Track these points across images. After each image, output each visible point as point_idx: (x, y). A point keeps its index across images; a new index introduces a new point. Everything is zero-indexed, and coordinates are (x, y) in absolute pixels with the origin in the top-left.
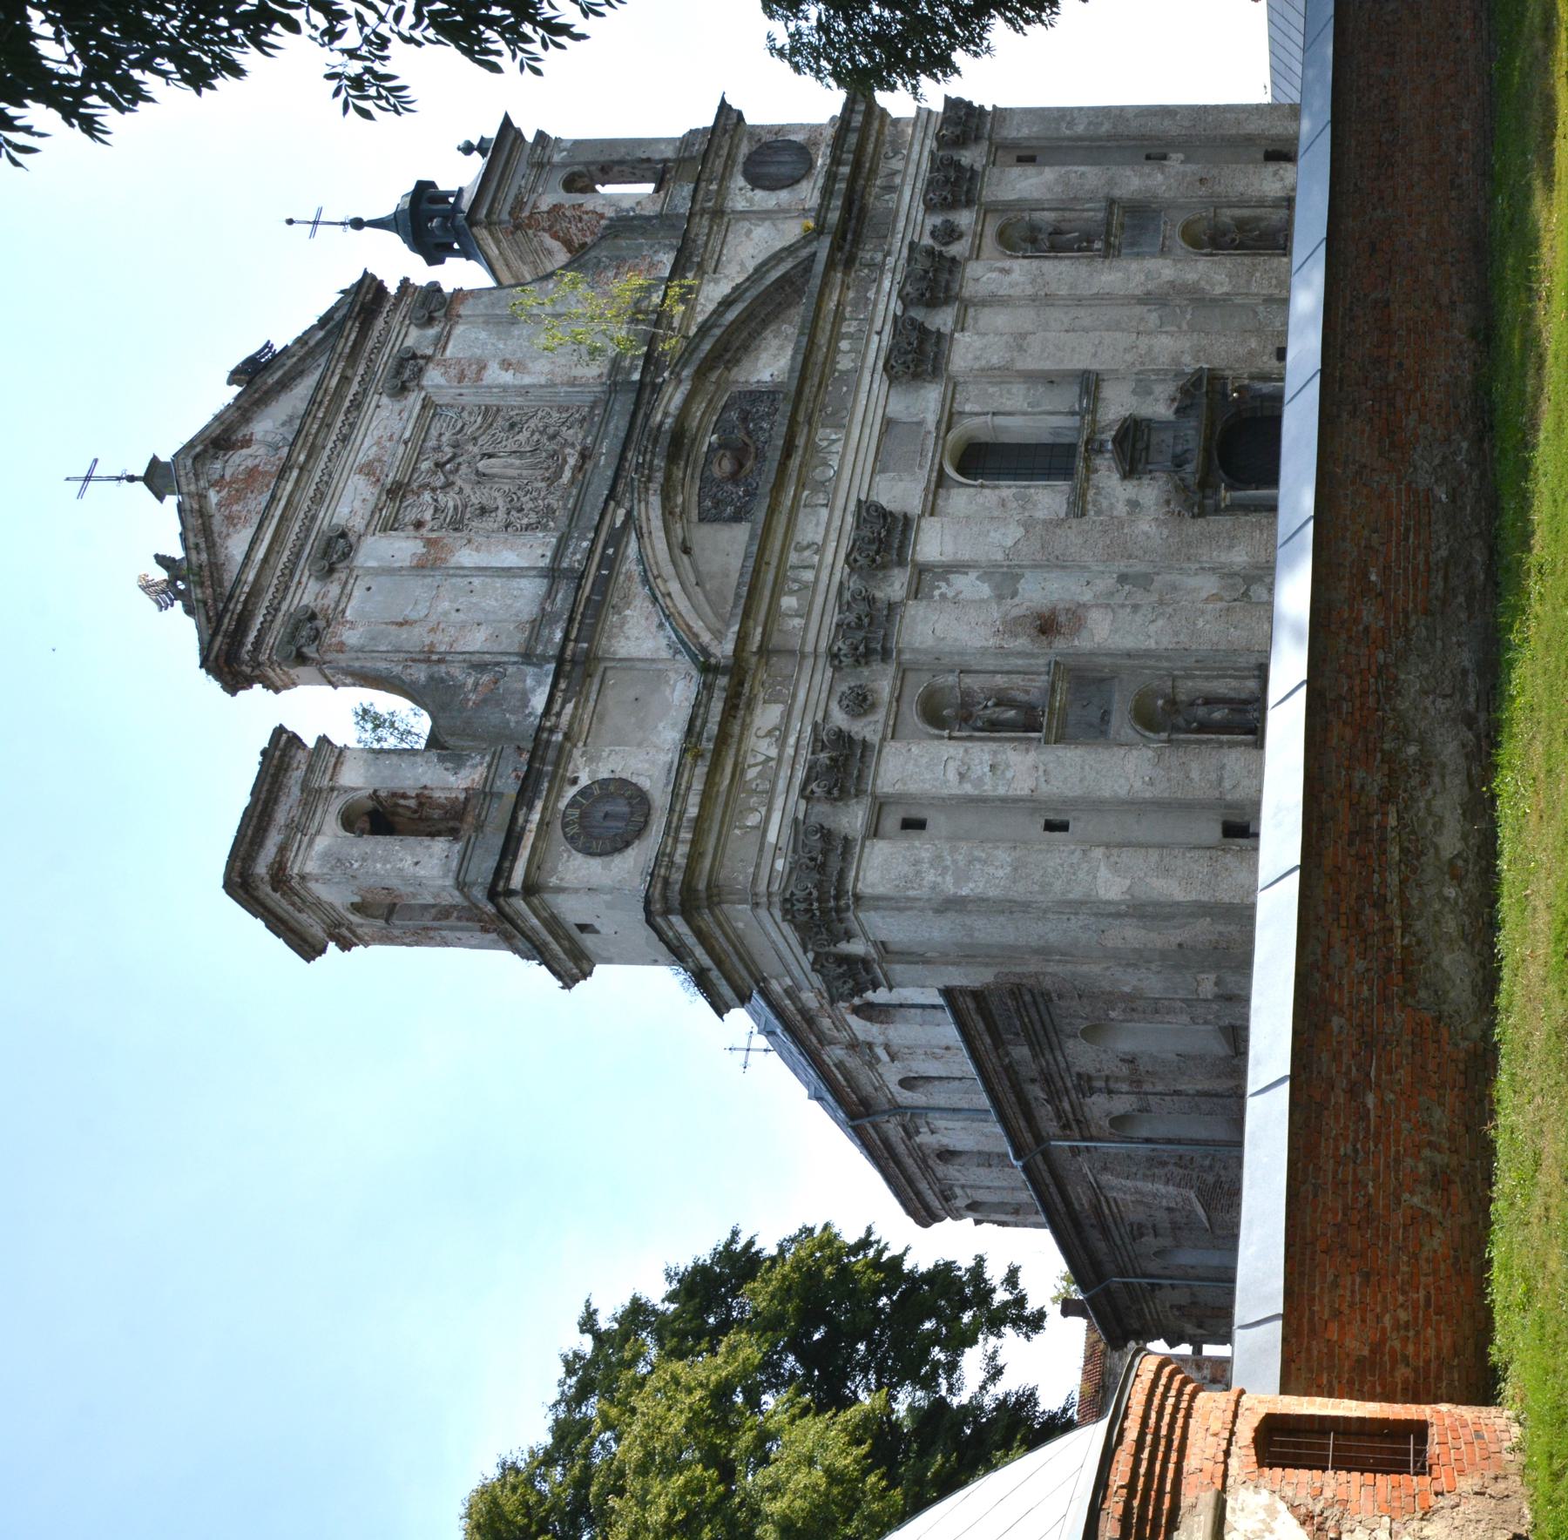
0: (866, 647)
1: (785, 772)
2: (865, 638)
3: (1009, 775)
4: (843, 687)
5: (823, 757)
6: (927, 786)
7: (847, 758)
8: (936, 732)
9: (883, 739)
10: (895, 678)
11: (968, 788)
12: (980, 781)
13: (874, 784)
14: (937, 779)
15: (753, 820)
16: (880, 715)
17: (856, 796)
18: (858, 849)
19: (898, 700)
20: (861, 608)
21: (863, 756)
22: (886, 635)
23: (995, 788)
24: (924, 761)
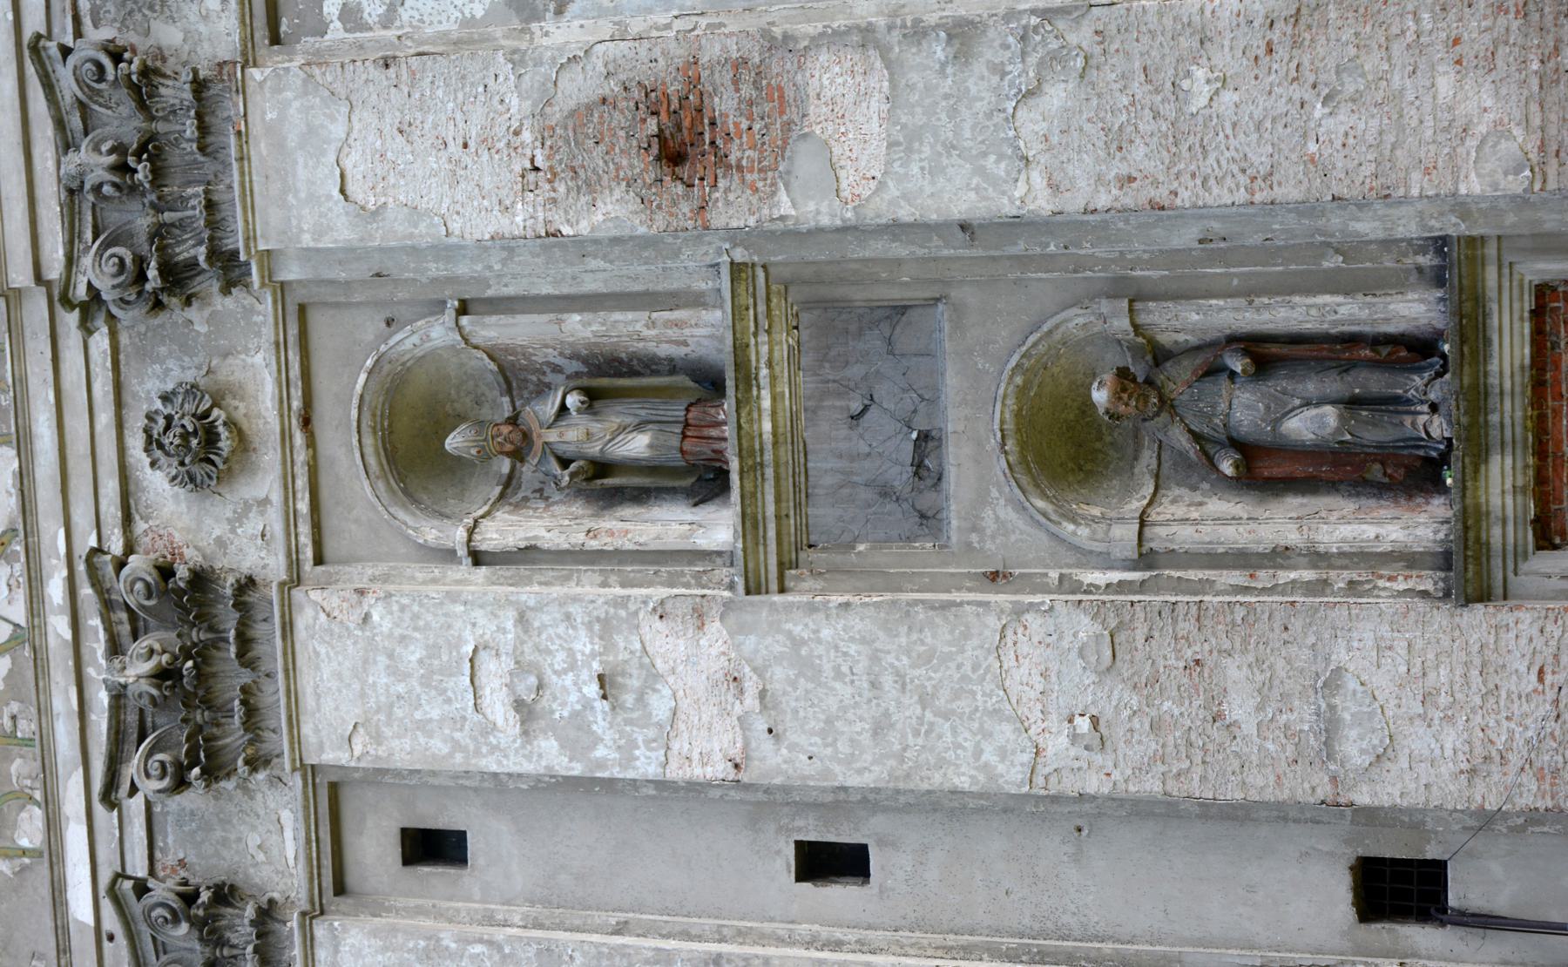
0: (166, 269)
1: (63, 699)
2: (159, 233)
3: (660, 706)
4: (147, 389)
5: (137, 670)
6: (439, 746)
7: (202, 655)
8: (431, 532)
9: (295, 579)
10: (280, 346)
11: (550, 756)
12: (577, 733)
13: (296, 741)
14: (459, 721)
15: (29, 831)
16: (265, 482)
17: (254, 764)
18: (297, 952)
19: (306, 422)
20: (121, 120)
21: (245, 642)
22: (210, 206)
23: (627, 751)
24: (413, 655)
